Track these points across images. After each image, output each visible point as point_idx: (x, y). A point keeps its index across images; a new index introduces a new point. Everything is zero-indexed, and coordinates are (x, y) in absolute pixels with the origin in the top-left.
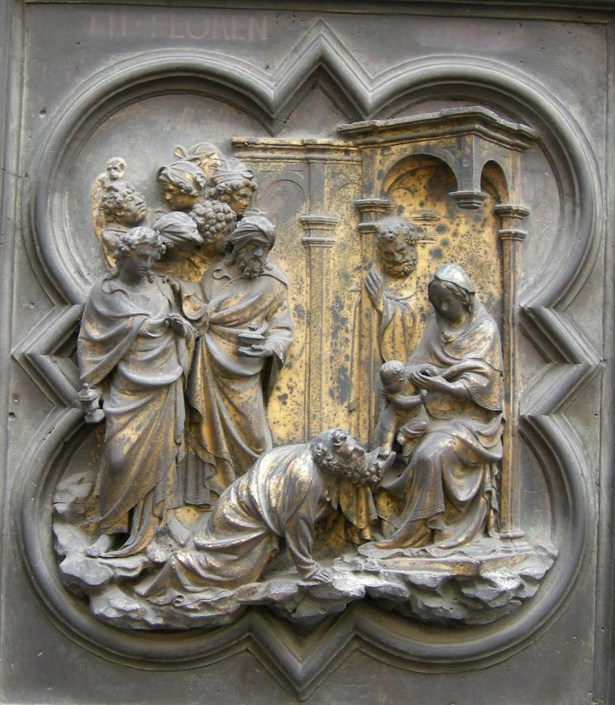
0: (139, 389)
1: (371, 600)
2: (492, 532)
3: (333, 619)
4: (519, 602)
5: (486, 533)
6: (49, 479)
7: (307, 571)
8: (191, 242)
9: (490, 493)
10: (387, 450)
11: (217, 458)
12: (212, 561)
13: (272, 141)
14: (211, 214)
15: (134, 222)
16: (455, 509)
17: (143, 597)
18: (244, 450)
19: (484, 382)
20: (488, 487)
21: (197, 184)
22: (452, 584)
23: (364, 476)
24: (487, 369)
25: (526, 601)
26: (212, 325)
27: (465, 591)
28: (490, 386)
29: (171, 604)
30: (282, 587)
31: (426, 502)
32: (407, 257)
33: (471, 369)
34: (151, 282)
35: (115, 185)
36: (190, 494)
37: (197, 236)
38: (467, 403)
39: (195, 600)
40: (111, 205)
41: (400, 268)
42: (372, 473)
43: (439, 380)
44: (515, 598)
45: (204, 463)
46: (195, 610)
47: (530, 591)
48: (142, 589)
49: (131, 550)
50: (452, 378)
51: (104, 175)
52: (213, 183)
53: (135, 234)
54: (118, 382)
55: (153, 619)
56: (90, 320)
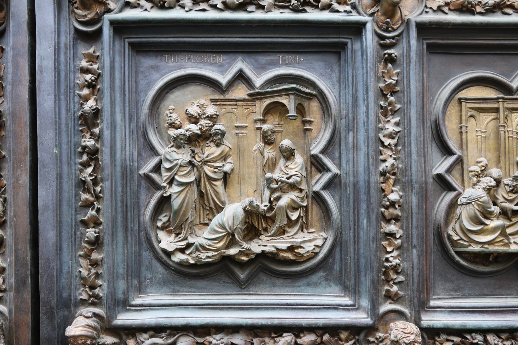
0: (181, 184)
1: (263, 254)
2: (305, 230)
3: (251, 262)
4: (313, 254)
5: (302, 231)
6: (154, 217)
7: (242, 245)
8: (197, 134)
9: (302, 217)
10: (267, 203)
11: (210, 207)
12: (210, 242)
13: (222, 97)
14: (204, 125)
15: (179, 127)
16: (291, 223)
17: (189, 254)
18: (219, 206)
19: (299, 179)
20: (302, 215)
21: (199, 114)
22: (291, 249)
23: (260, 213)
24: (299, 175)
25: (317, 254)
26: (205, 162)
27: (296, 251)
28: (301, 180)
29: (197, 257)
30: (233, 251)
31: (281, 221)
32: (272, 138)
33: (295, 175)
34: (184, 148)
35: (171, 115)
36: (202, 220)
37: (199, 132)
38: (293, 187)
39: (204, 256)
40: (170, 122)
41: (270, 141)
42: (262, 212)
43: (284, 179)
44: (312, 252)
45: (206, 209)
46: (204, 259)
47: (317, 250)
48: (188, 252)
49: (184, 238)
50: (288, 178)
51: (168, 112)
52: (204, 114)
53: (179, 132)
54: (175, 183)
55: (192, 262)
56: (165, 162)
